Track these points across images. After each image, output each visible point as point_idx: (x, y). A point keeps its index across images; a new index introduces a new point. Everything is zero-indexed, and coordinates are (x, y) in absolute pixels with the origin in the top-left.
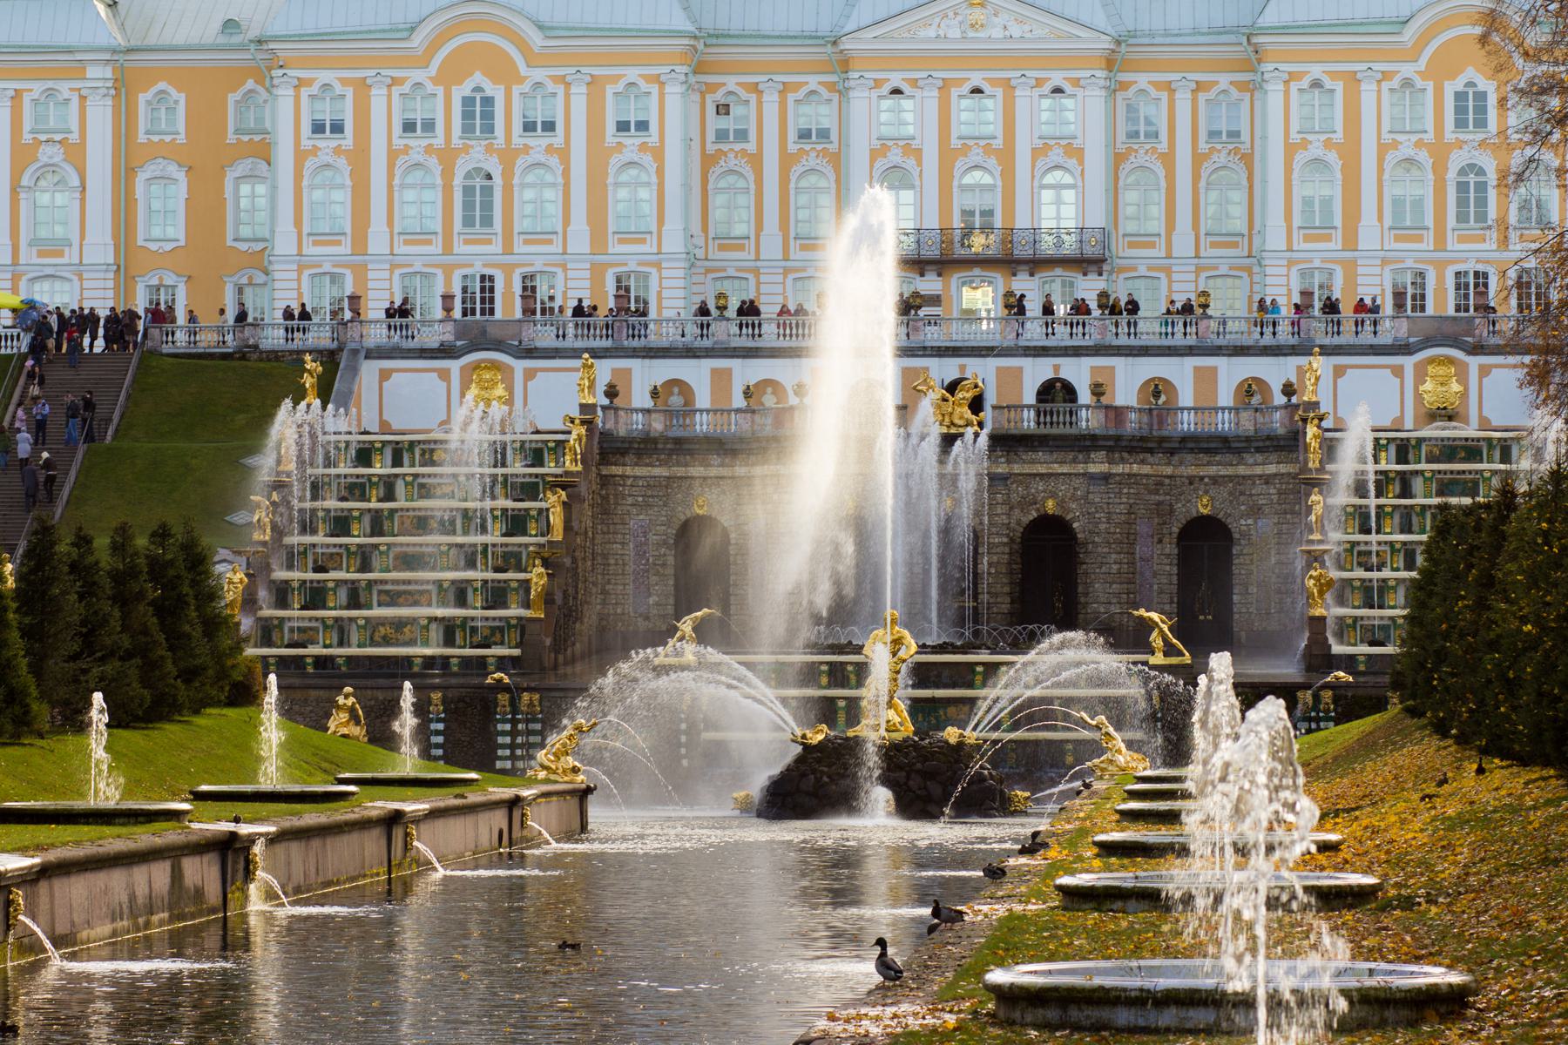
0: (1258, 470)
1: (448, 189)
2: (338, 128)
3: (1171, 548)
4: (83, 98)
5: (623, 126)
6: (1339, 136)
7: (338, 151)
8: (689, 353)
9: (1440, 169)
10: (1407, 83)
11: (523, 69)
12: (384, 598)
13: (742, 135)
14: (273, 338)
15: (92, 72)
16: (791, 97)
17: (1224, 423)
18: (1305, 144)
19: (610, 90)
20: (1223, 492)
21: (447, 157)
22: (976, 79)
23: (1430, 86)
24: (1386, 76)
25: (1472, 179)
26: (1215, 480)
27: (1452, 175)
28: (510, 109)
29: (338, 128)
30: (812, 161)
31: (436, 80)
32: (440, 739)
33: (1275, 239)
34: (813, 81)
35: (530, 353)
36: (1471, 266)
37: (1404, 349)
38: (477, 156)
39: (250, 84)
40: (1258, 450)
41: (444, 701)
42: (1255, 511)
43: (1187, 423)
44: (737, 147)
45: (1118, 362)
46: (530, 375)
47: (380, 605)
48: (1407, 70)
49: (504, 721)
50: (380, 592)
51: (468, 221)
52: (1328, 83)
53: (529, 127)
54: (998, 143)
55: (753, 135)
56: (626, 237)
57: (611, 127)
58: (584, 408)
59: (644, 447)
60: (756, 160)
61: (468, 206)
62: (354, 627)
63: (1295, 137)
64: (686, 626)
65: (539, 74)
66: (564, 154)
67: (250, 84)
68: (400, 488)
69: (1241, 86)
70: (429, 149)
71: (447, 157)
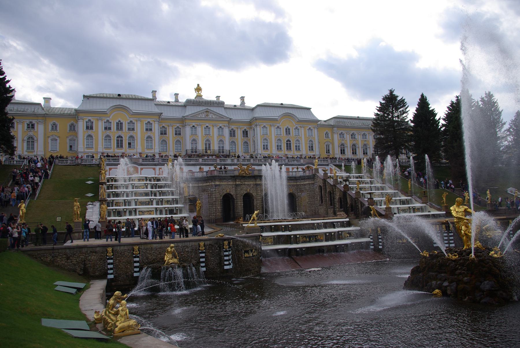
0: (302, 183)
10: (278, 127)
12: (141, 213)
13: (165, 134)
22: (207, 125)
26: (293, 185)
35: (142, 165)
37: (304, 165)
38: (120, 133)
40: (302, 179)
41: (204, 245)
42: (302, 191)
47: (139, 215)
49: (226, 251)
51: (118, 146)
55: (167, 133)
56: (148, 148)
61: (118, 143)
62: (137, 221)
66: (137, 133)
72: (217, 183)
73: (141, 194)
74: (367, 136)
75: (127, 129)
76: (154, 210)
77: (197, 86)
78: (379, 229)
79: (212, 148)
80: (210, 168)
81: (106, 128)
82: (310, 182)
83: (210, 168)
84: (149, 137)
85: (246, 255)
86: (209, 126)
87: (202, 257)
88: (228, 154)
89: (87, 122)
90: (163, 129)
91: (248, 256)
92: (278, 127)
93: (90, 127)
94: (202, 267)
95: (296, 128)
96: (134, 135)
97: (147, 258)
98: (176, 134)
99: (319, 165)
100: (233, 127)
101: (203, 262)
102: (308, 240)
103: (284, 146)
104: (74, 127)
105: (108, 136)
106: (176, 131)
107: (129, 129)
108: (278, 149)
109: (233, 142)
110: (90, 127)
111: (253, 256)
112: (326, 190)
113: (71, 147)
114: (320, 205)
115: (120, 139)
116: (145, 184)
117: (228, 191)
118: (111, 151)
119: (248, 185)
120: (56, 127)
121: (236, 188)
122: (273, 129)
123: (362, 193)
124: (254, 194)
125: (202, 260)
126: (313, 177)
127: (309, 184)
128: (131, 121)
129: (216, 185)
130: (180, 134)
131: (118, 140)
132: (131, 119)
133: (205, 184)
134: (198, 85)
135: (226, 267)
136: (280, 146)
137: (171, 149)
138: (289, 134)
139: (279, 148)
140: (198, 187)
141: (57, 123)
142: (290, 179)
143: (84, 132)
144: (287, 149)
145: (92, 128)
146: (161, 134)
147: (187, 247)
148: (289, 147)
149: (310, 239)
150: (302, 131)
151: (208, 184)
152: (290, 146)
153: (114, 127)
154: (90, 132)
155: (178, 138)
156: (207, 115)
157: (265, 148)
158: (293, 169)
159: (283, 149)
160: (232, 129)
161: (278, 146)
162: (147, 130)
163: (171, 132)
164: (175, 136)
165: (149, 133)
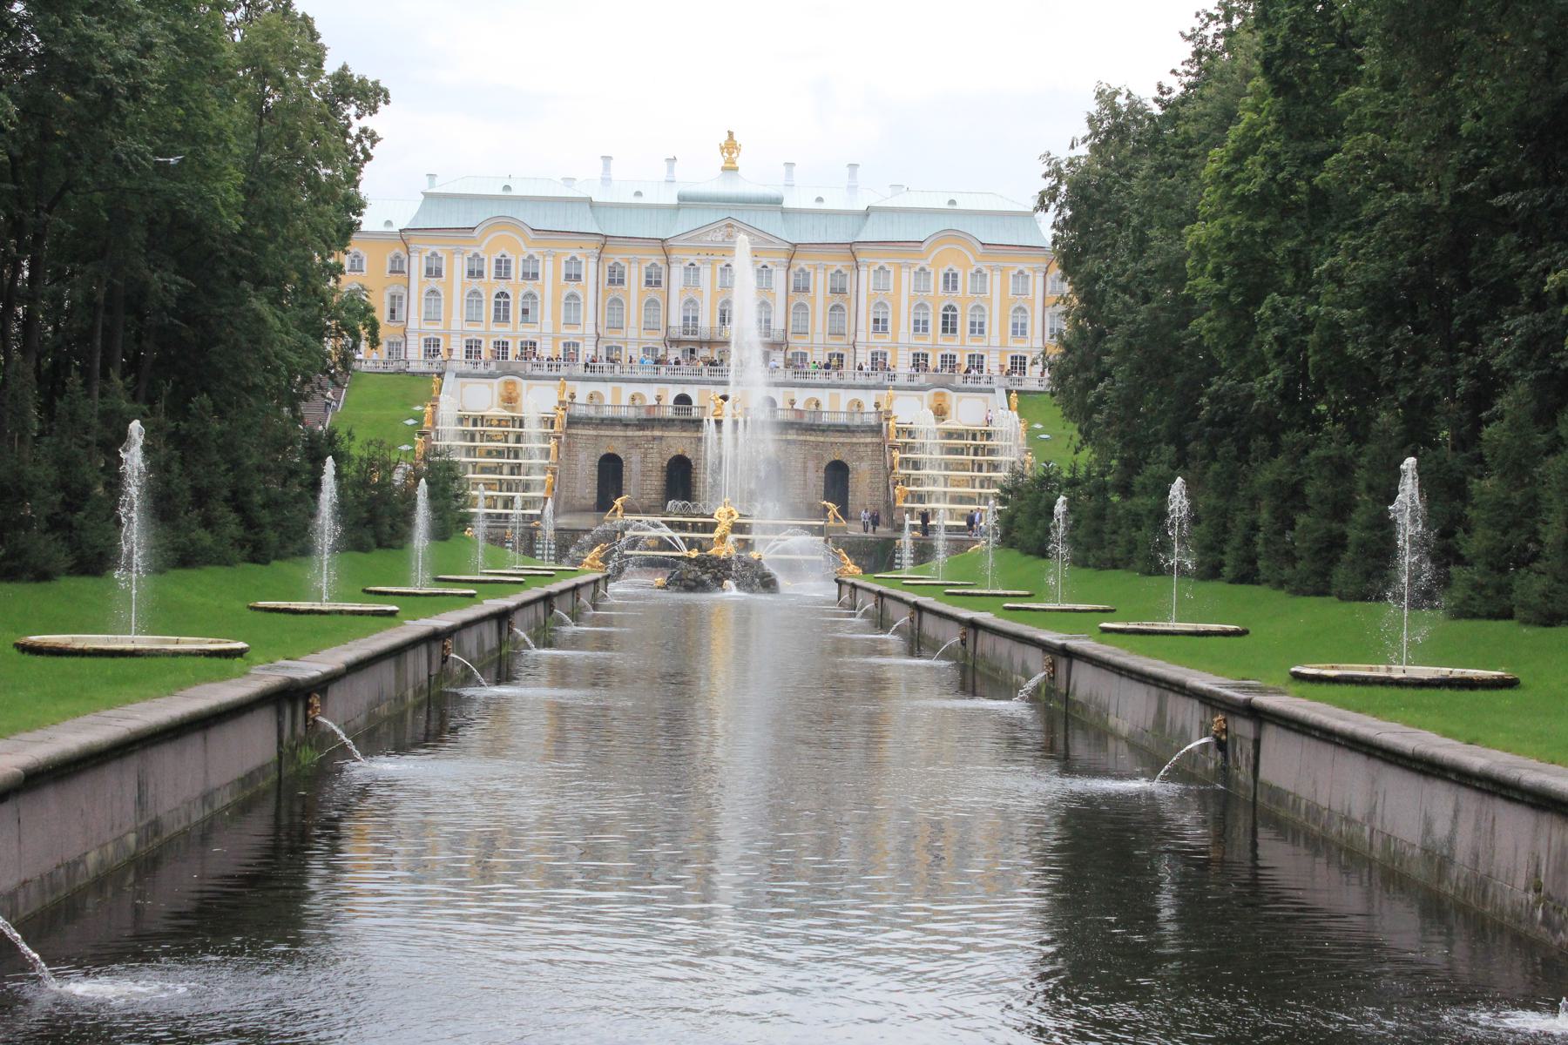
1: (488, 301)
3: (822, 474)
8: (604, 380)
10: (922, 269)
13: (621, 282)
14: (414, 367)
17: (842, 419)
20: (846, 449)
27: (941, 312)
30: (653, 296)
33: (861, 337)
35: (530, 377)
36: (948, 352)
38: (502, 286)
42: (861, 459)
43: (826, 419)
45: (796, 390)
46: (529, 387)
51: (497, 318)
58: (561, 402)
59: (587, 422)
60: (628, 292)
61: (497, 310)
64: (618, 502)
66: (542, 287)
68: (478, 437)
72: (657, 433)
73: (489, 453)
77: (726, 137)
81: (471, 273)
84: (573, 296)
88: (778, 338)
92: (922, 269)
93: (433, 272)
95: (979, 271)
96: (536, 292)
98: (648, 283)
100: (803, 264)
103: (935, 323)
104: (402, 262)
105: (475, 293)
106: (649, 276)
107: (525, 275)
108: (916, 330)
109: (801, 305)
110: (433, 272)
115: (502, 300)
118: (482, 328)
120: (361, 261)
122: (907, 278)
128: (531, 257)
129: (654, 438)
131: (498, 304)
132: (532, 251)
134: (731, 134)
136: (925, 322)
137: (633, 321)
138: (955, 288)
139: (920, 326)
141: (362, 253)
143: (421, 282)
144: (945, 330)
145: (439, 274)
146: (611, 282)
148: (949, 325)
150: (995, 280)
153: (490, 269)
154: (433, 283)
155: (653, 293)
156: (730, 236)
157: (879, 325)
160: (802, 270)
161: (916, 322)
162: (568, 277)
163: (635, 277)
165: (572, 287)
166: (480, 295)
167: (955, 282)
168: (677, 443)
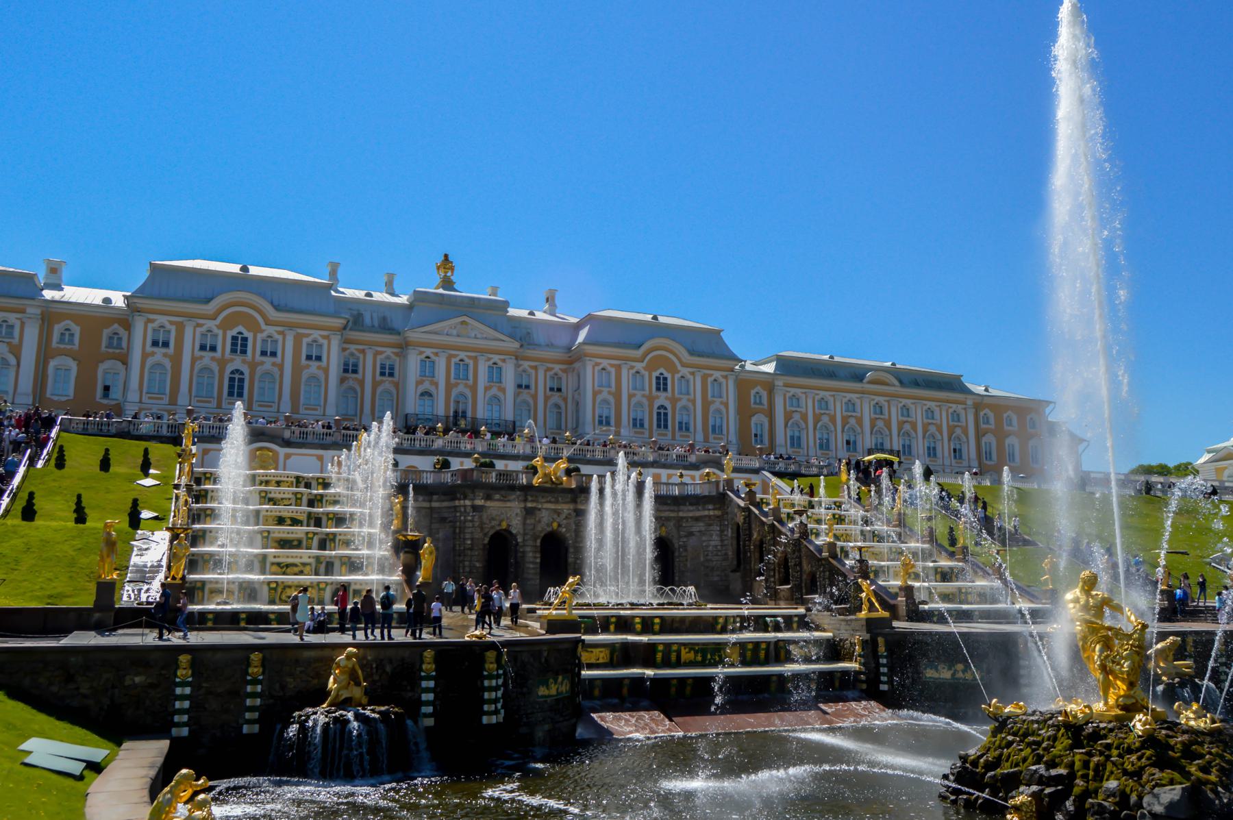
0: (691, 514)
2: (166, 344)
4: (23, 324)
5: (309, 358)
6: (613, 389)
7: (165, 355)
9: (651, 406)
11: (263, 327)
12: (275, 568)
13: (355, 371)
15: (29, 310)
16: (379, 357)
18: (600, 392)
19: (305, 341)
21: (222, 363)
23: (646, 374)
24: (632, 367)
25: (662, 411)
26: (668, 519)
27: (656, 407)
28: (255, 345)
29: (166, 344)
31: (218, 327)
32: (431, 696)
33: (588, 428)
34: (389, 351)
35: (287, 443)
38: (237, 363)
39: (116, 326)
40: (691, 504)
44: (354, 376)
46: (288, 456)
48: (639, 366)
49: (490, 677)
50: (273, 564)
52: (609, 369)
53: (264, 353)
54: (471, 382)
57: (304, 357)
60: (362, 383)
63: (597, 388)
65: (271, 330)
66: (281, 367)
67: (116, 326)
69: (564, 371)
70: (213, 359)
71: (222, 363)
72: (479, 502)
73: (281, 521)
74: (858, 408)
75: (258, 352)
76: (312, 561)
78: (880, 640)
79: (469, 414)
80: (462, 464)
82: (711, 513)
83: (462, 464)
84: (313, 377)
85: (542, 691)
86: (467, 360)
87: (427, 690)
89: (154, 330)
90: (351, 361)
91: (546, 692)
94: (426, 715)
97: (283, 687)
98: (382, 374)
99: (736, 470)
101: (427, 703)
102: (699, 658)
103: (650, 419)
106: (383, 367)
108: (635, 425)
111: (558, 693)
112: (750, 535)
113: (107, 388)
114: (734, 571)
115: (237, 376)
116: (295, 494)
117: (504, 525)
119: (555, 511)
120: (72, 335)
121: (525, 519)
123: (842, 548)
124: (570, 536)
125: (425, 697)
126: (720, 500)
127: (709, 516)
130: (391, 375)
133: (446, 504)
134: (446, 256)
135: (485, 720)
138: (665, 390)
140: (431, 508)
142: (660, 500)
144: (659, 426)
146: (346, 371)
147: (391, 661)
149: (704, 657)
151: (457, 503)
152: (666, 420)
158: (669, 476)
159: (646, 425)
160: (524, 371)
161: (635, 420)
162: (309, 358)
164: (378, 378)
166: (211, 371)
167: (665, 384)
168: (508, 514)
